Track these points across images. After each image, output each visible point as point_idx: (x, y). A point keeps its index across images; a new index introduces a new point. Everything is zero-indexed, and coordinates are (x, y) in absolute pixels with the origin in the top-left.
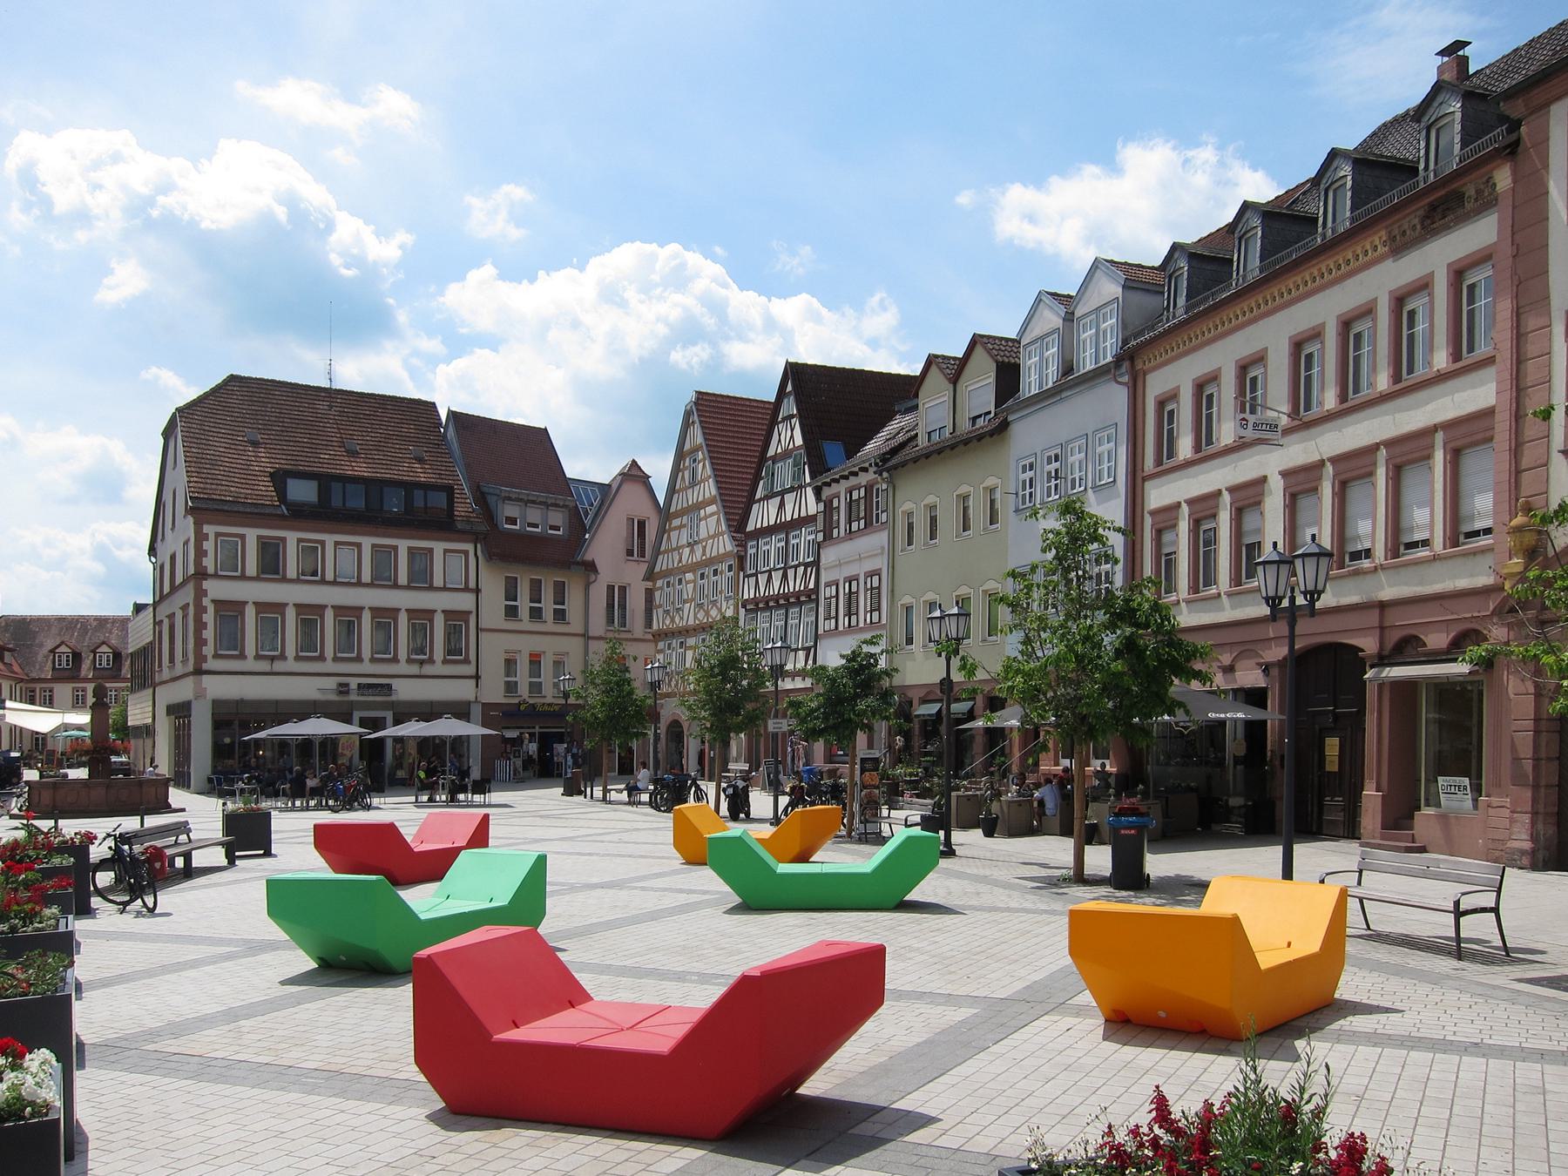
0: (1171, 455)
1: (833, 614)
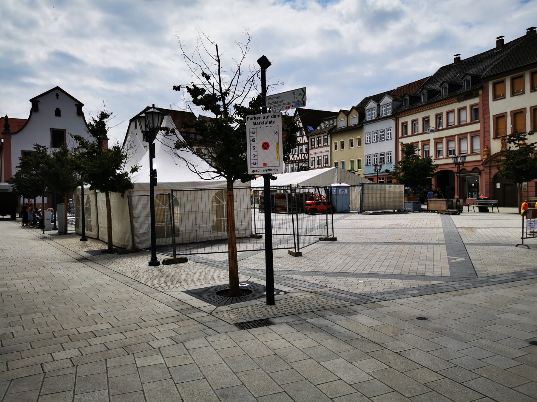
0: (407, 134)
1: (314, 164)
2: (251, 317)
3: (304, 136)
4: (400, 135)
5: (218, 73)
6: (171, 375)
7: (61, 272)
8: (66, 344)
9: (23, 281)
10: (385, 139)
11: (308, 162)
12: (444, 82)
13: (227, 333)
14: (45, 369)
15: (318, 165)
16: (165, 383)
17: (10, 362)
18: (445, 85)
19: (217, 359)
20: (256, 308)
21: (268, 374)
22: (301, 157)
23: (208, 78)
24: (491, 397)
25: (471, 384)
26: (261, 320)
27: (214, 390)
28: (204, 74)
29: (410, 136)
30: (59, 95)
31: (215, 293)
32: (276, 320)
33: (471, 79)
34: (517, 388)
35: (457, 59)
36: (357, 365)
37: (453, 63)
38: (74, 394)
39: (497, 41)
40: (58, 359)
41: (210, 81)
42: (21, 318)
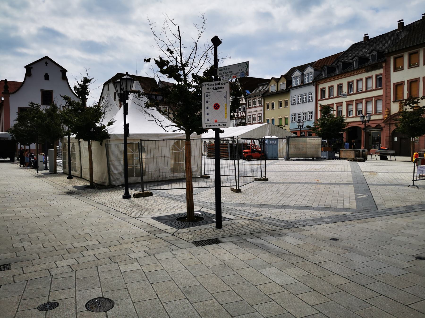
0: (324, 97)
1: (250, 120)
2: (205, 237)
3: (242, 98)
4: (319, 98)
5: (179, 49)
6: (147, 278)
7: (55, 202)
8: (66, 255)
9: (26, 208)
10: (307, 101)
11: (246, 118)
12: (355, 56)
13: (187, 249)
14: (51, 272)
15: (253, 122)
16: (143, 283)
17: (25, 268)
18: (356, 59)
19: (181, 267)
20: (208, 231)
21: (219, 277)
22: (240, 115)
23: (172, 52)
24: (385, 295)
25: (370, 286)
26: (212, 240)
27: (180, 288)
28: (168, 50)
29: (327, 99)
30: (47, 63)
31: (176, 219)
32: (223, 240)
33: (376, 54)
34: (405, 289)
35: (366, 37)
36: (286, 272)
37: (363, 41)
38: (76, 291)
39: (398, 24)
40: (61, 266)
41: (173, 55)
42: (29, 236)
